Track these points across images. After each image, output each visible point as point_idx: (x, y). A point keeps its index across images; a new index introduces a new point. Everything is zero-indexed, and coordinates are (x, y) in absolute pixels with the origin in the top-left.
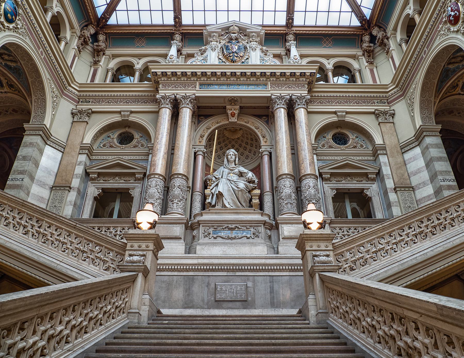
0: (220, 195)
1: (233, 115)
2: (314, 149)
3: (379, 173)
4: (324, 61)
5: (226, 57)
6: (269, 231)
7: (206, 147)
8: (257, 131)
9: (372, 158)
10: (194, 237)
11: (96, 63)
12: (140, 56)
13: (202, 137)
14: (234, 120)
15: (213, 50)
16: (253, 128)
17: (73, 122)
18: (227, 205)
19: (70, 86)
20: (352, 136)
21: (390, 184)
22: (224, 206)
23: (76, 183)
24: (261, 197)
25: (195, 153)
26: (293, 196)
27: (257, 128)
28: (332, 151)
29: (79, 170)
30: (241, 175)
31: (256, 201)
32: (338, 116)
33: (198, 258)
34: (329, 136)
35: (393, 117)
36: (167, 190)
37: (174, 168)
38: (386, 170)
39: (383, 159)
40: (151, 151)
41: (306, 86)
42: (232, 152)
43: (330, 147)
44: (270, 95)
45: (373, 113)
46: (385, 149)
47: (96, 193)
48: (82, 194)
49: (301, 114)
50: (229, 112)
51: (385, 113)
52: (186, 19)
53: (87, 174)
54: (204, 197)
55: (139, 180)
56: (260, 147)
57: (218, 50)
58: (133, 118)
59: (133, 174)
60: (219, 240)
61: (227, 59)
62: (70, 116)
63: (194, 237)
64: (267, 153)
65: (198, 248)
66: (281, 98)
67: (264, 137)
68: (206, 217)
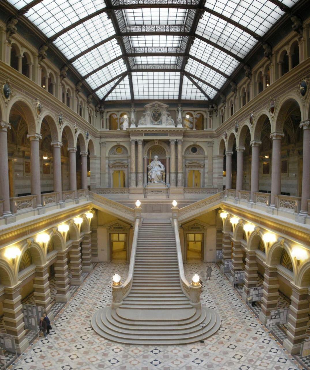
0: (153, 179)
1: (156, 143)
2: (184, 157)
3: (204, 166)
4: (192, 113)
5: (153, 119)
6: (167, 191)
7: (147, 156)
8: (165, 148)
9: (203, 159)
10: (146, 192)
11: (102, 117)
12: (118, 112)
13: (146, 151)
14: (156, 144)
15: (148, 116)
16: (164, 147)
17: (101, 147)
18: (155, 182)
19: (97, 133)
20: (198, 149)
21: (206, 170)
22: (154, 182)
23: (107, 171)
24: (166, 175)
25: (144, 158)
26: (175, 179)
27: (165, 147)
28: (191, 155)
29: (107, 166)
30: (160, 166)
31: (164, 177)
32: (194, 143)
33: (148, 200)
34: (190, 149)
35: (213, 144)
36: (137, 177)
37: (138, 170)
38: (206, 166)
39: (206, 161)
40: (129, 157)
41: (182, 135)
42: (156, 157)
43: (190, 154)
44: (168, 139)
45: (207, 141)
46: (207, 157)
47: (113, 172)
48: (109, 173)
49: (179, 147)
50: (155, 142)
51: (211, 142)
52: (136, 98)
53: (109, 166)
54: (148, 176)
55: (126, 168)
56: (166, 156)
57: (151, 115)
58: (121, 144)
59: (124, 166)
60: (153, 194)
61: (154, 120)
62: (99, 145)
63: (146, 192)
64: (168, 158)
65: (148, 197)
66: (173, 140)
67: (167, 151)
68: (149, 187)
